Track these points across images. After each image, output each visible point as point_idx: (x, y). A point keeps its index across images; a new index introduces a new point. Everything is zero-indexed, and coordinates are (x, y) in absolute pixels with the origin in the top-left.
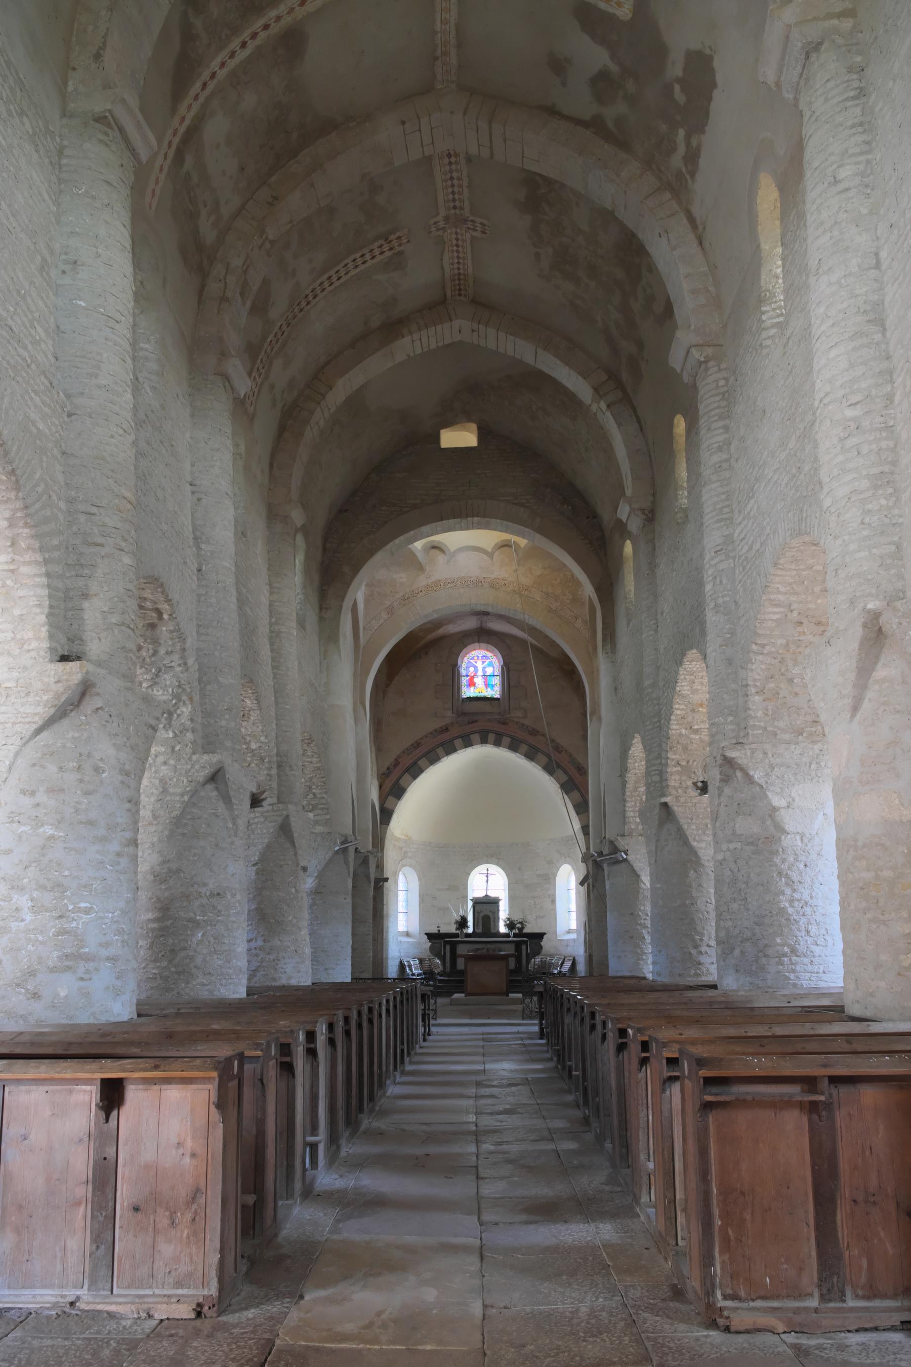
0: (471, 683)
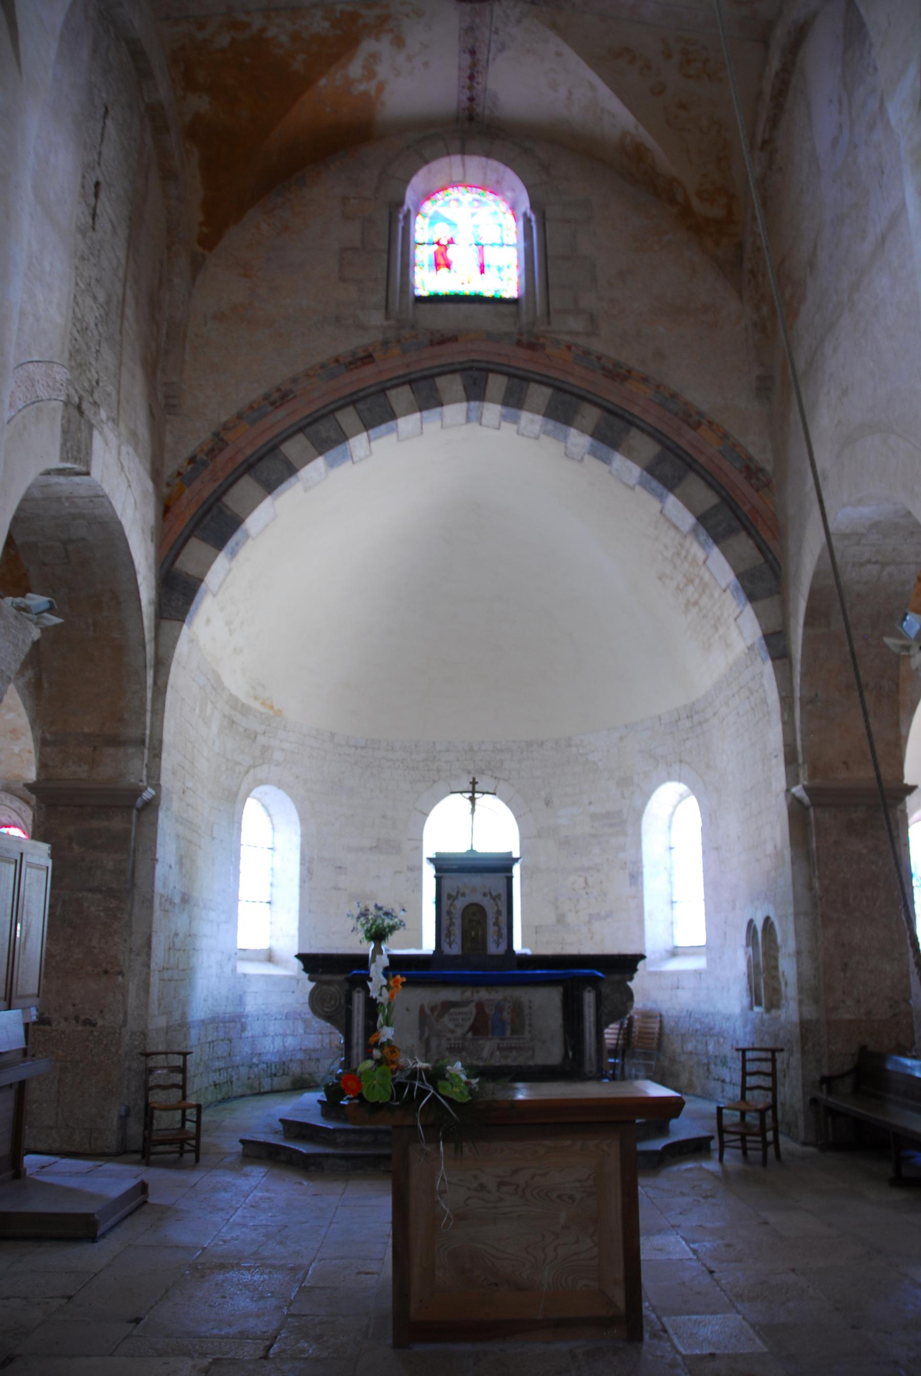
0: (441, 262)
